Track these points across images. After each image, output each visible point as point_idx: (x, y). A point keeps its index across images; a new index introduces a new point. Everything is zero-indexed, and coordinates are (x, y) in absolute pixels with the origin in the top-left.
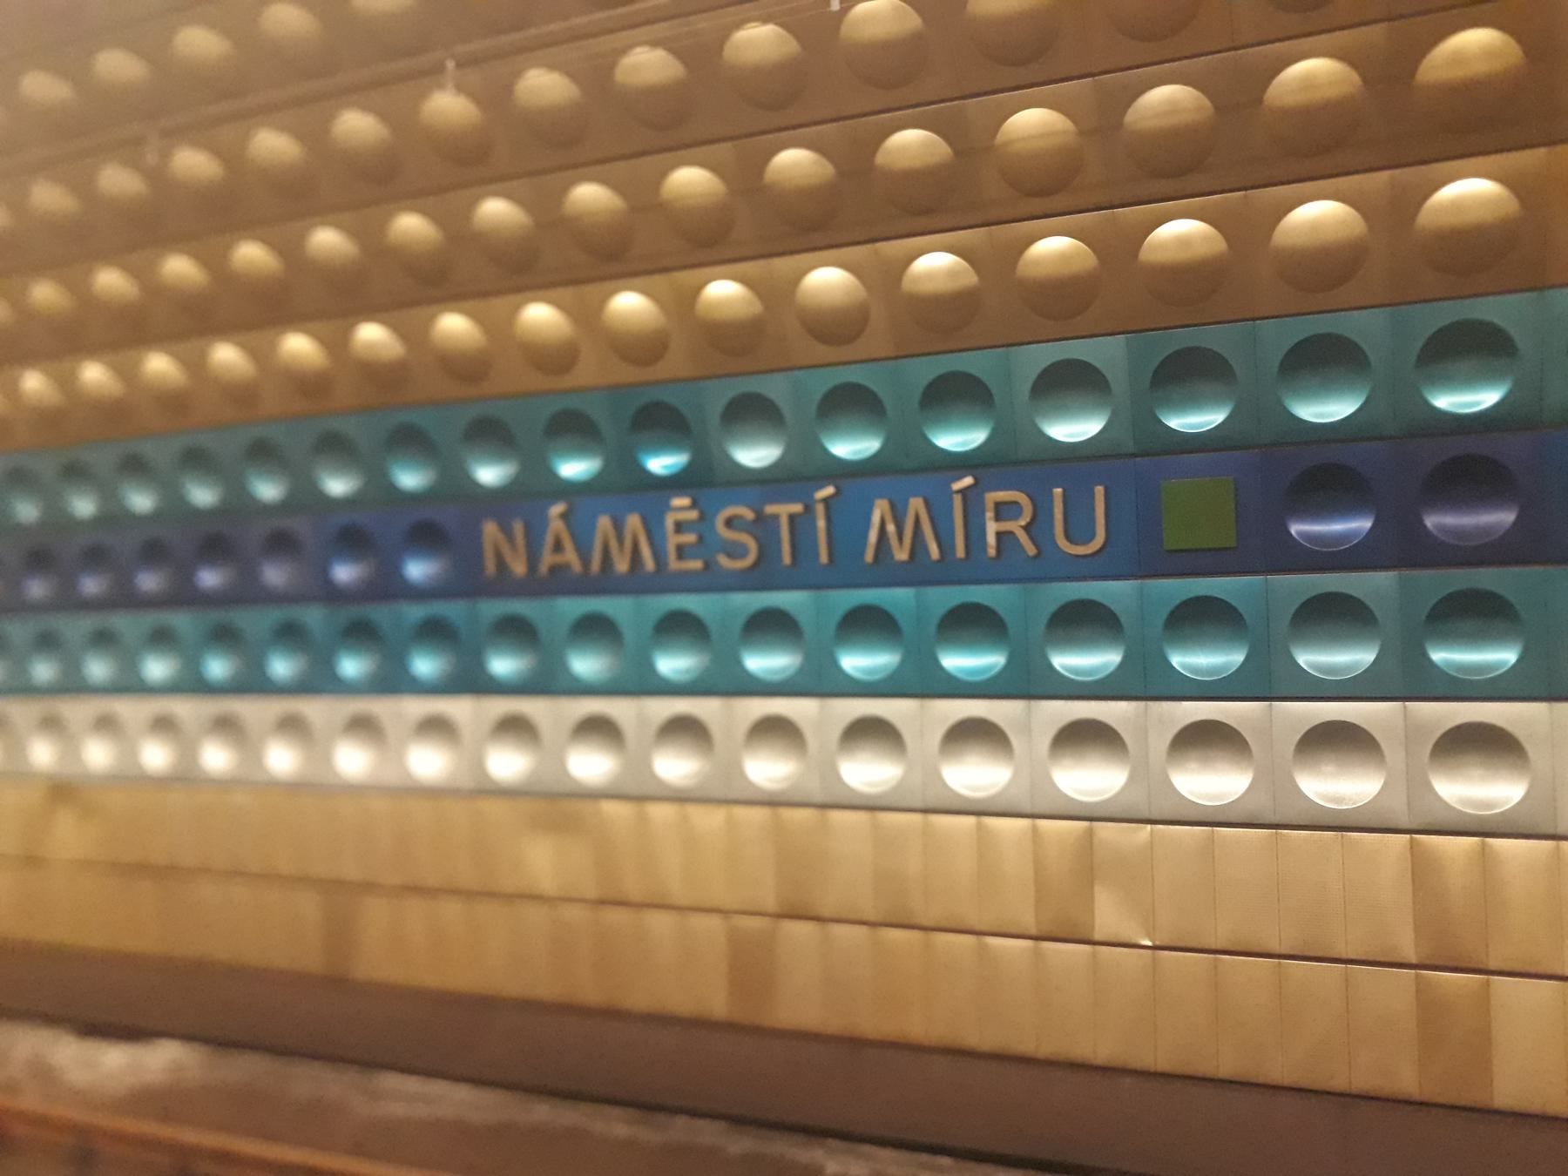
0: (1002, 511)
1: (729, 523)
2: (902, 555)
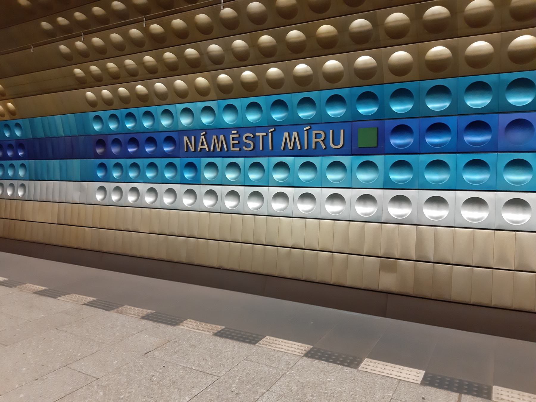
1: (246, 138)
2: (290, 147)
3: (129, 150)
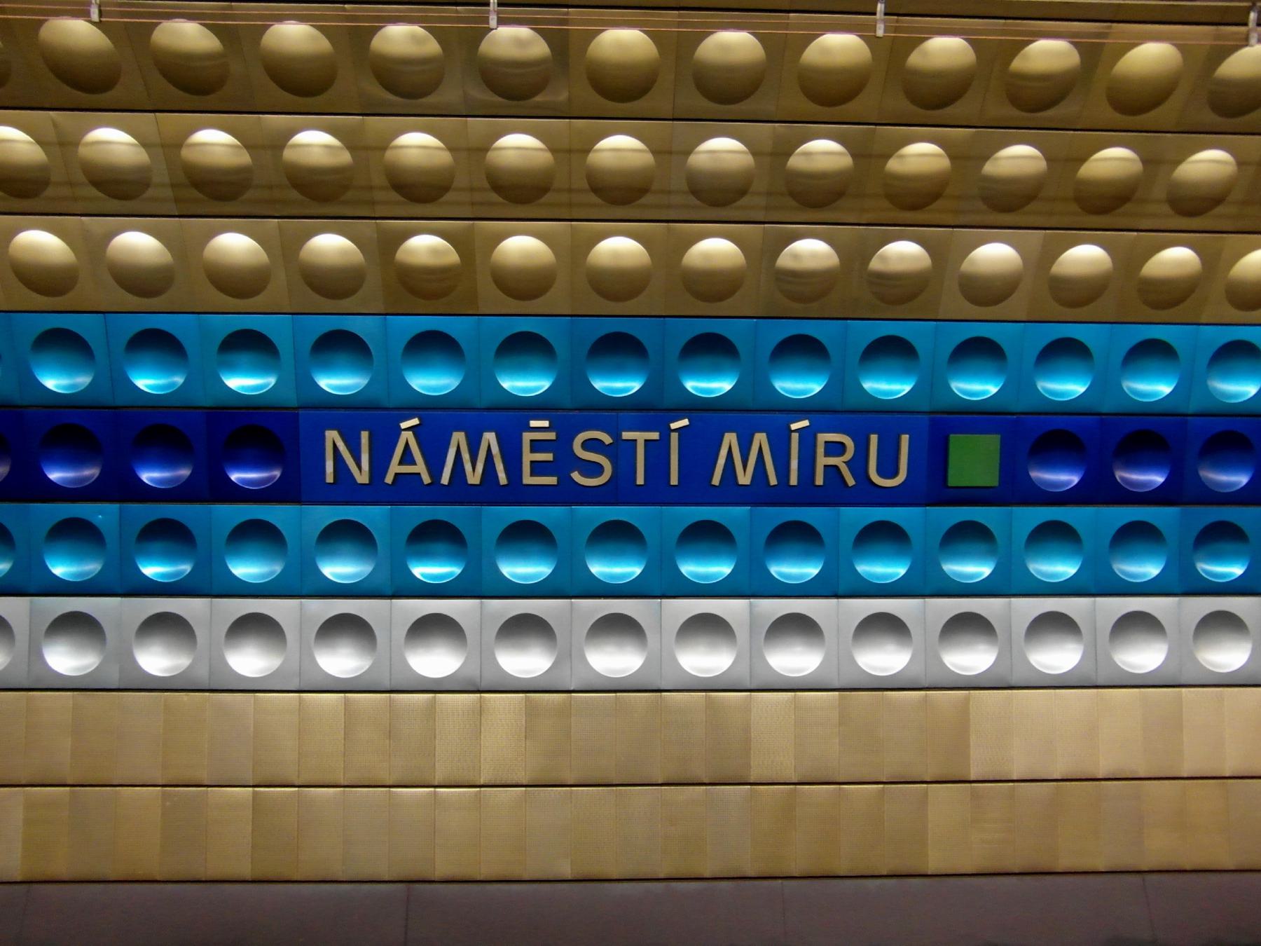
0: (835, 449)
1: (587, 445)
3: (235, 476)
